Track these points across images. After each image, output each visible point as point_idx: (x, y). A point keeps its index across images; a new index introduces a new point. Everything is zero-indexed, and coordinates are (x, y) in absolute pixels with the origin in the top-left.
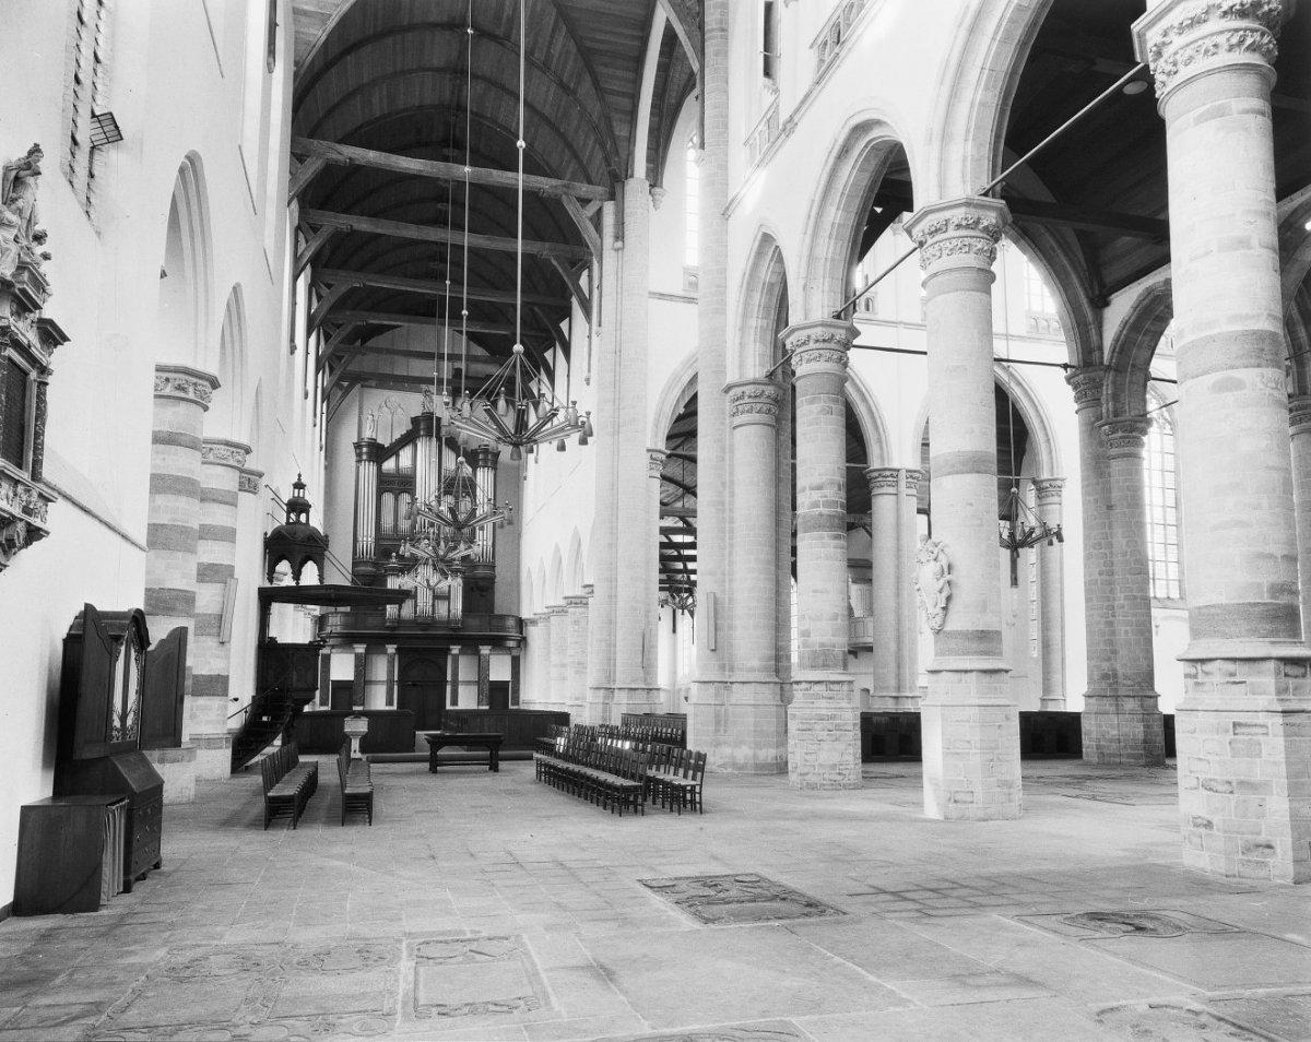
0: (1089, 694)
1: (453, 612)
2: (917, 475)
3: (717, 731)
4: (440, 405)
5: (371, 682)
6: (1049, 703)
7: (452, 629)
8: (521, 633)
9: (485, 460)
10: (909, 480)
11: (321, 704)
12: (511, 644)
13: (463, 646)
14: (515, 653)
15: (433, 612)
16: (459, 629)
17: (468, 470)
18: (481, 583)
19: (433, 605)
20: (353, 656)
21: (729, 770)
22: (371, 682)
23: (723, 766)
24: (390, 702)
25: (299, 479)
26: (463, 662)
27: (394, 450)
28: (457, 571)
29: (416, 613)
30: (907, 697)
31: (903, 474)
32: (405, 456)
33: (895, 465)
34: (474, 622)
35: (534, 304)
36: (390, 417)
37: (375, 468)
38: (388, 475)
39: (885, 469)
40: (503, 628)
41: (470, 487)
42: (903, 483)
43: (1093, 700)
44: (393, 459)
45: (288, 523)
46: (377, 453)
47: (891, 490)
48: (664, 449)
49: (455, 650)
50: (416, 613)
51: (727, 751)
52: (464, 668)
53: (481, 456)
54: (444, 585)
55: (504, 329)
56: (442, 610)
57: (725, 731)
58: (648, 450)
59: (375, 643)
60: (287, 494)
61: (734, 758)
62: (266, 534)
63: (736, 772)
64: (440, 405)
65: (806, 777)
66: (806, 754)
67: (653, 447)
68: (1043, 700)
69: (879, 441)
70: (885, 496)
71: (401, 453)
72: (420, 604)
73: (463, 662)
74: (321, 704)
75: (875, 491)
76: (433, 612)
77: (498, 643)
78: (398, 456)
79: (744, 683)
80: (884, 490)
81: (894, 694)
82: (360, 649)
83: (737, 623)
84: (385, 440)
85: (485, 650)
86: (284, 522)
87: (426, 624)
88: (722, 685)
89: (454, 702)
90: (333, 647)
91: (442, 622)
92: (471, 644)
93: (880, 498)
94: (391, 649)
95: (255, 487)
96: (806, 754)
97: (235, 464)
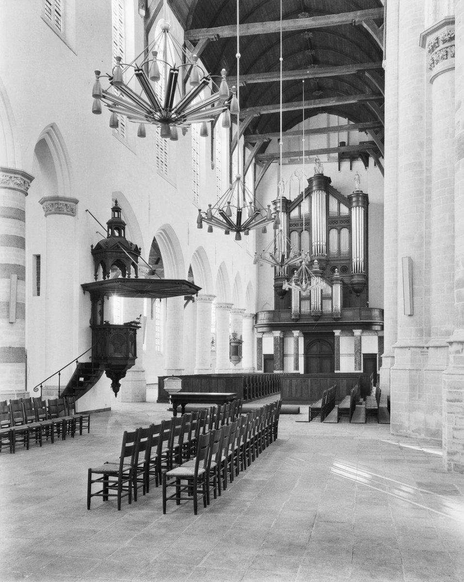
1: (334, 307)
3: (412, 396)
4: (330, 168)
5: (287, 355)
7: (335, 319)
9: (357, 201)
11: (258, 369)
13: (342, 331)
14: (380, 334)
15: (322, 309)
16: (339, 319)
17: (344, 210)
18: (356, 287)
19: (322, 304)
21: (423, 436)
22: (287, 355)
23: (418, 431)
24: (297, 368)
25: (116, 205)
27: (298, 202)
28: (337, 279)
29: (310, 309)
32: (305, 204)
34: (349, 313)
35: (363, 71)
36: (298, 182)
37: (285, 216)
38: (295, 220)
40: (370, 317)
41: (347, 222)
44: (297, 209)
45: (108, 237)
46: (288, 205)
49: (337, 332)
50: (310, 309)
51: (420, 416)
52: (345, 345)
53: (354, 199)
54: (328, 290)
55: (354, 99)
56: (327, 308)
57: (420, 397)
59: (287, 329)
60: (107, 215)
61: (426, 423)
62: (92, 246)
63: (429, 438)
64: (330, 168)
65: (456, 458)
66: (455, 429)
71: (302, 204)
72: (313, 303)
74: (258, 369)
76: (322, 309)
77: (367, 327)
78: (300, 207)
79: (437, 347)
82: (277, 333)
83: (434, 286)
84: (292, 198)
85: (357, 332)
86: (106, 236)
87: (319, 316)
88: (418, 350)
90: (263, 333)
91: (327, 315)
92: (348, 328)
94: (296, 333)
95: (72, 210)
96: (455, 429)
97: (16, 187)
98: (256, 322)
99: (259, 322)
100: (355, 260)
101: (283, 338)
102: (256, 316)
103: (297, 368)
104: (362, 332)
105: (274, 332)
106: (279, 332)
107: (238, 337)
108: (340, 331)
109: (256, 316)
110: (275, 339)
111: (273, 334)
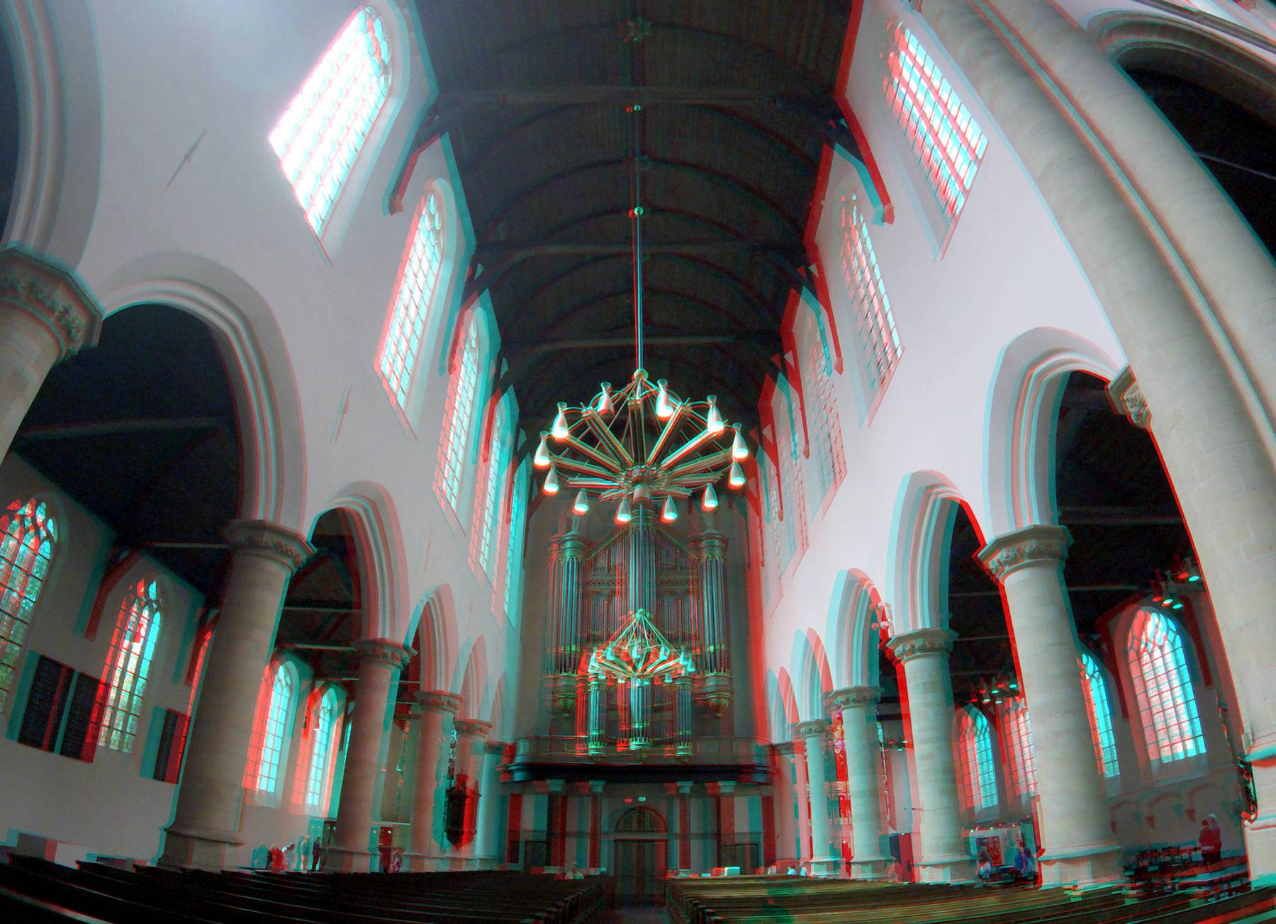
8: (774, 763)
12: (760, 778)
20: (545, 799)
24: (595, 862)
26: (695, 806)
73: (695, 806)
82: (556, 785)
85: (726, 787)
89: (686, 863)
98: (512, 762)
99: (518, 759)
100: (712, 648)
101: (565, 799)
102: (512, 750)
103: (595, 862)
104: (734, 786)
105: (548, 781)
106: (561, 782)
107: (470, 785)
108: (690, 784)
109: (512, 750)
110: (552, 798)
111: (547, 785)
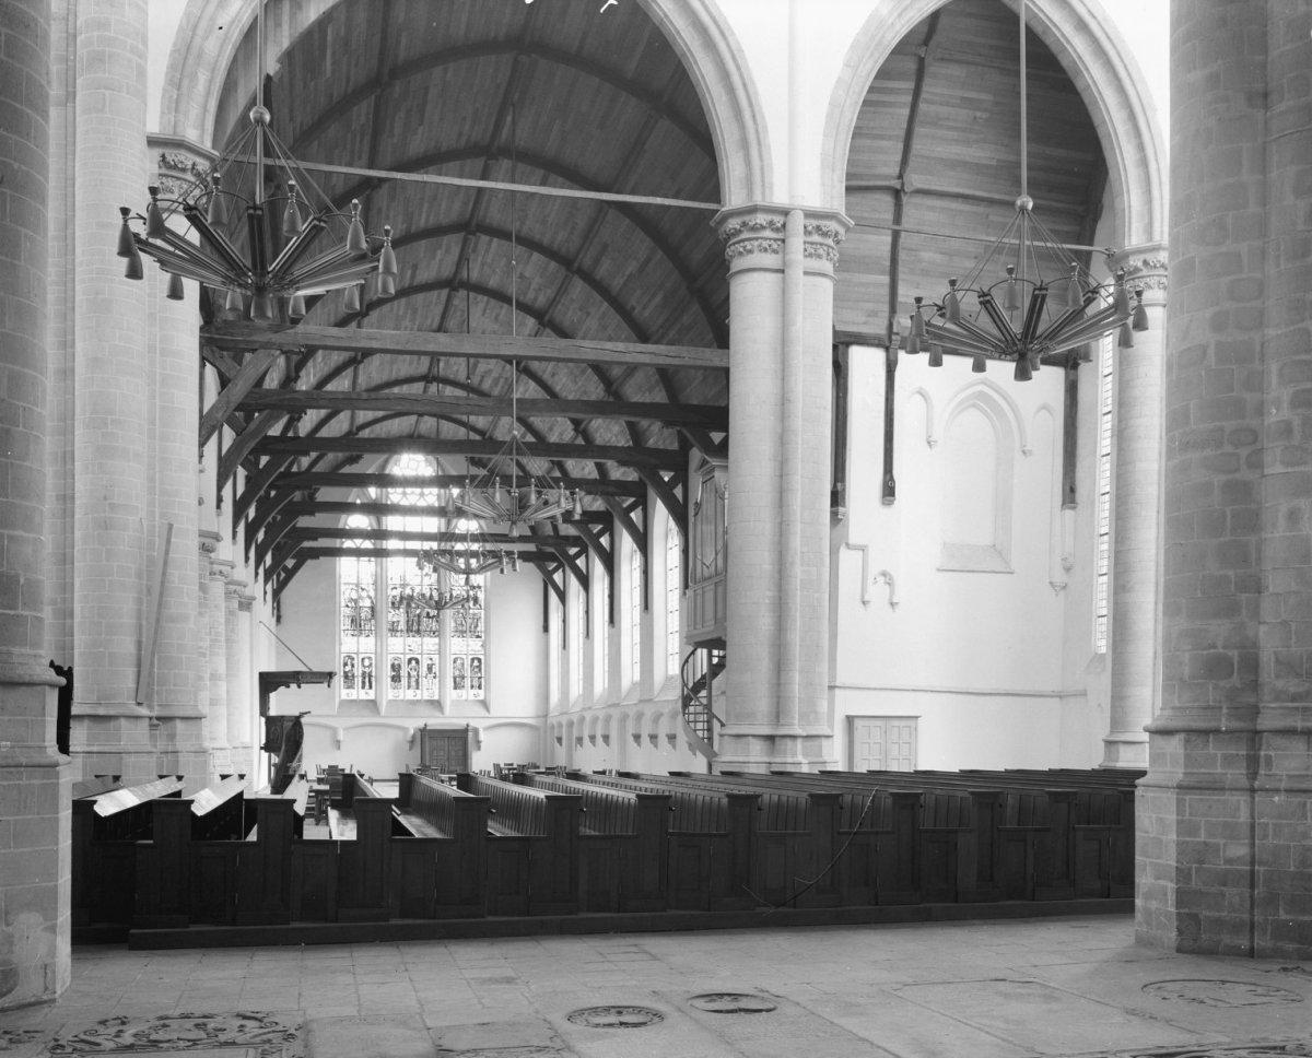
0: (1161, 724)
2: (833, 226)
6: (1122, 748)
10: (816, 238)
30: (794, 737)
31: (798, 222)
33: (779, 198)
39: (753, 210)
42: (797, 242)
43: (1175, 745)
47: (770, 260)
48: (207, 145)
58: (153, 142)
67: (168, 134)
68: (1109, 743)
69: (744, 144)
70: (755, 275)
75: (737, 264)
80: (758, 259)
81: (767, 731)
93: (746, 278)
